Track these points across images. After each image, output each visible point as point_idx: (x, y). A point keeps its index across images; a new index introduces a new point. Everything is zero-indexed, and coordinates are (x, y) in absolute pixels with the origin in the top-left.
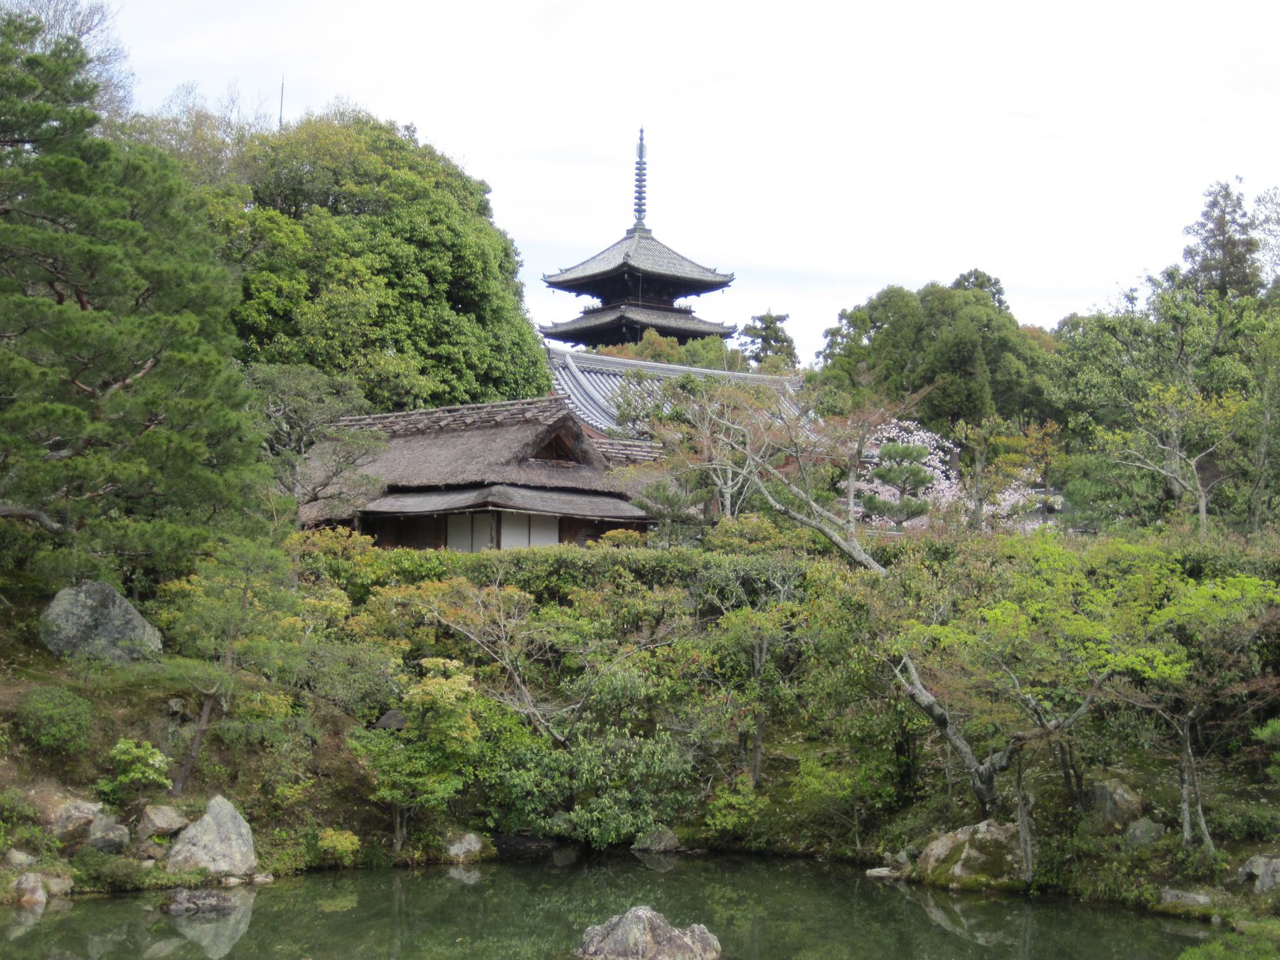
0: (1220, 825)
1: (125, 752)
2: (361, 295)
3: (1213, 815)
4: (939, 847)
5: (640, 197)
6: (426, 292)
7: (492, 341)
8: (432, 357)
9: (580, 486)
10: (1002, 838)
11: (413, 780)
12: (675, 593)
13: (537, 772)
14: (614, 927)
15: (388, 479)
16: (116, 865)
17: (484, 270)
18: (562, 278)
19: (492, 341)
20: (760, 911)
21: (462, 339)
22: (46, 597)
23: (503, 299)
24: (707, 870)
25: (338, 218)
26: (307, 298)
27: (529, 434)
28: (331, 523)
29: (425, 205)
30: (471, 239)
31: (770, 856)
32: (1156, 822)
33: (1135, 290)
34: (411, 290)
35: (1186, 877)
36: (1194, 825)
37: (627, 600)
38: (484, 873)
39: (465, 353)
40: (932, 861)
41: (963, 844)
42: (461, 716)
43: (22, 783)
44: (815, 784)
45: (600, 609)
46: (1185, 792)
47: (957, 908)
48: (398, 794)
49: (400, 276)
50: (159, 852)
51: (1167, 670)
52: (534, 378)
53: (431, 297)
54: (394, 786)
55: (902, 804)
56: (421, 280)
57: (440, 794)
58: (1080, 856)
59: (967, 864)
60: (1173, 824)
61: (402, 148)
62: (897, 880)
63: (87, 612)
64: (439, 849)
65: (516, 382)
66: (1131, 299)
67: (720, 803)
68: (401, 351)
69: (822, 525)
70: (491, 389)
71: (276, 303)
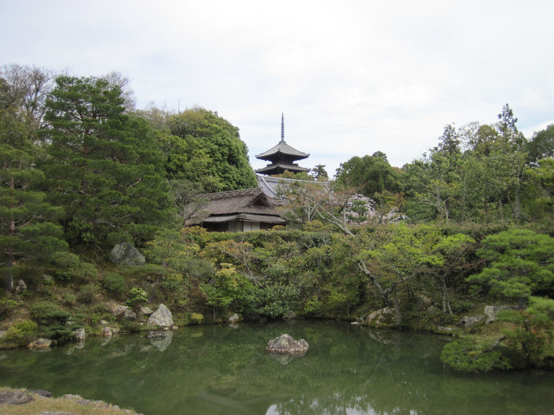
0: (454, 307)
1: (135, 291)
2: (203, 160)
3: (452, 304)
4: (372, 316)
5: (283, 132)
6: (221, 159)
7: (240, 172)
8: (223, 177)
9: (266, 213)
10: (391, 312)
11: (218, 299)
12: (294, 243)
13: (255, 295)
14: (277, 340)
15: (211, 212)
16: (132, 324)
17: (238, 152)
18: (260, 156)
19: (240, 172)
20: (320, 335)
21: (232, 172)
22: (112, 247)
23: (243, 160)
24: (304, 323)
25: (196, 138)
26: (187, 161)
27: (251, 199)
28: (194, 225)
29: (221, 134)
30: (234, 143)
31: (322, 319)
32: (435, 307)
33: (425, 153)
34: (217, 158)
35: (445, 323)
36: (447, 308)
37: (280, 245)
38: (239, 325)
39: (233, 176)
40: (370, 319)
41: (379, 315)
42: (232, 280)
43: (105, 301)
44: (336, 298)
45: (272, 248)
46: (444, 298)
47: (378, 333)
48: (214, 302)
49: (213, 154)
50: (145, 320)
51: (438, 262)
52: (253, 183)
53: (222, 160)
54: (213, 300)
55: (362, 303)
56: (219, 155)
57: (226, 303)
58: (413, 317)
59: (381, 320)
60: (440, 307)
61: (214, 118)
62: (360, 325)
63: (123, 251)
64: (227, 318)
65: (247, 184)
66: (425, 156)
67: (308, 304)
68: (214, 176)
69: (336, 223)
70: (240, 187)
71: (178, 163)
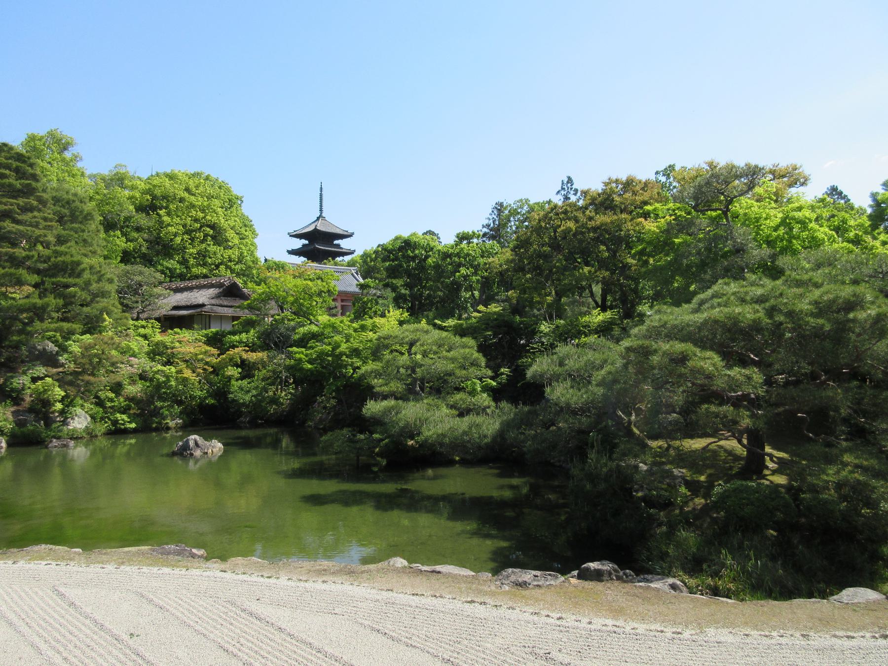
5: (321, 206)
